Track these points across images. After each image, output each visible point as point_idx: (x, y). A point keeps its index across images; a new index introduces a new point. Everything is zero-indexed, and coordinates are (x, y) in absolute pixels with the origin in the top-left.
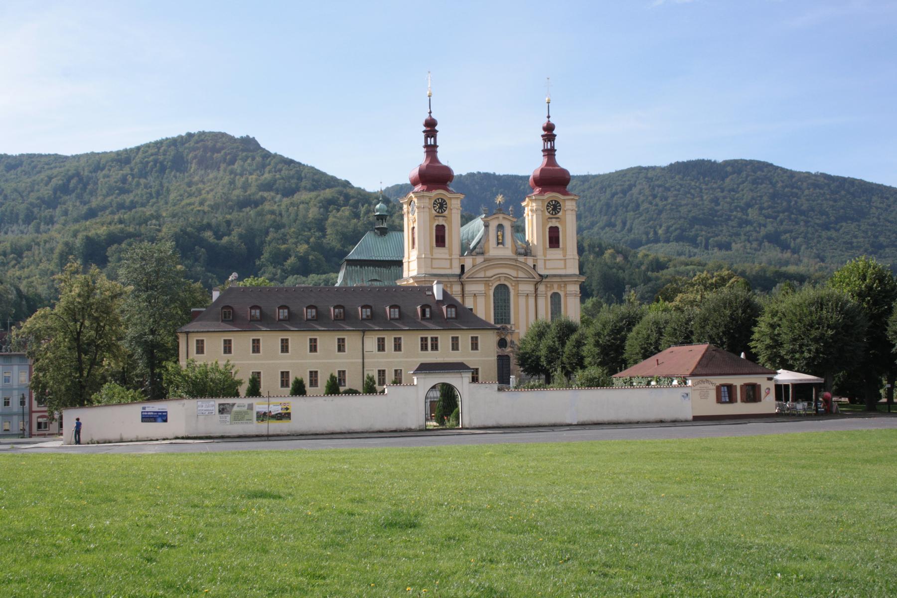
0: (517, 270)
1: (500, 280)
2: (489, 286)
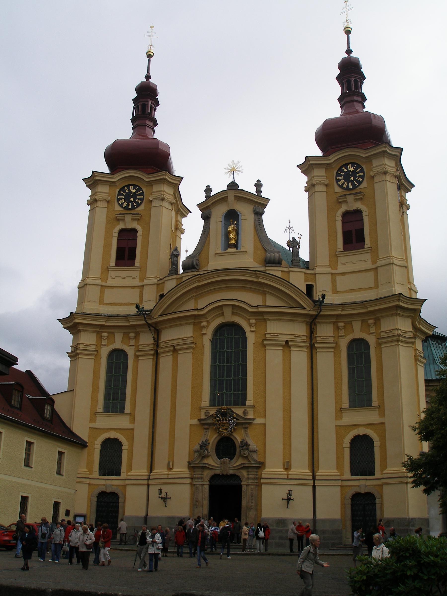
0: (264, 294)
1: (222, 314)
2: (202, 328)
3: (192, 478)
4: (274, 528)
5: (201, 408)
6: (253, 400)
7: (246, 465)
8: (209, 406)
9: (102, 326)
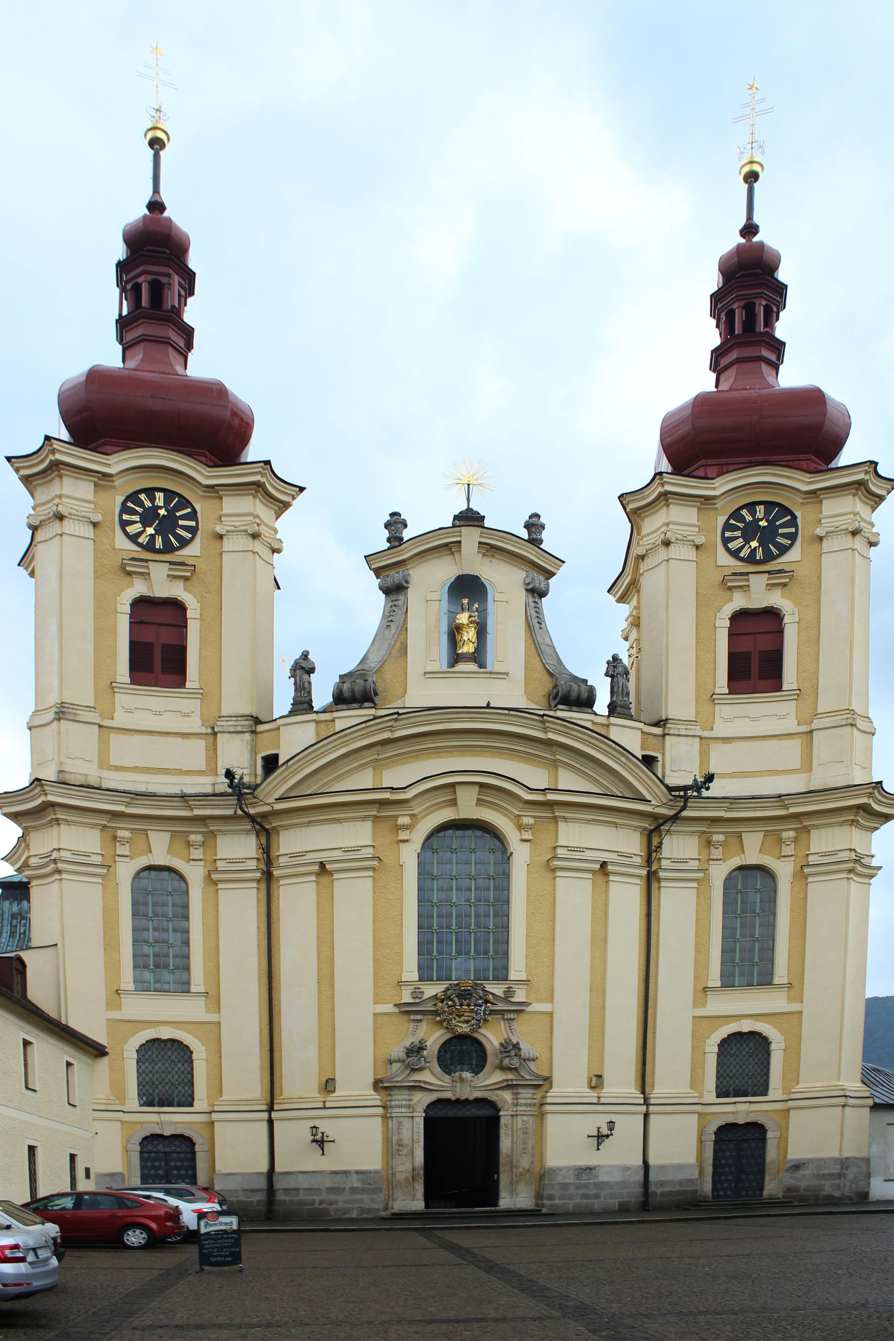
0: (555, 765)
3: (384, 1107)
4: (571, 1181)
5: (400, 984)
6: (526, 971)
7: (514, 1083)
8: (418, 980)
9: (115, 815)
